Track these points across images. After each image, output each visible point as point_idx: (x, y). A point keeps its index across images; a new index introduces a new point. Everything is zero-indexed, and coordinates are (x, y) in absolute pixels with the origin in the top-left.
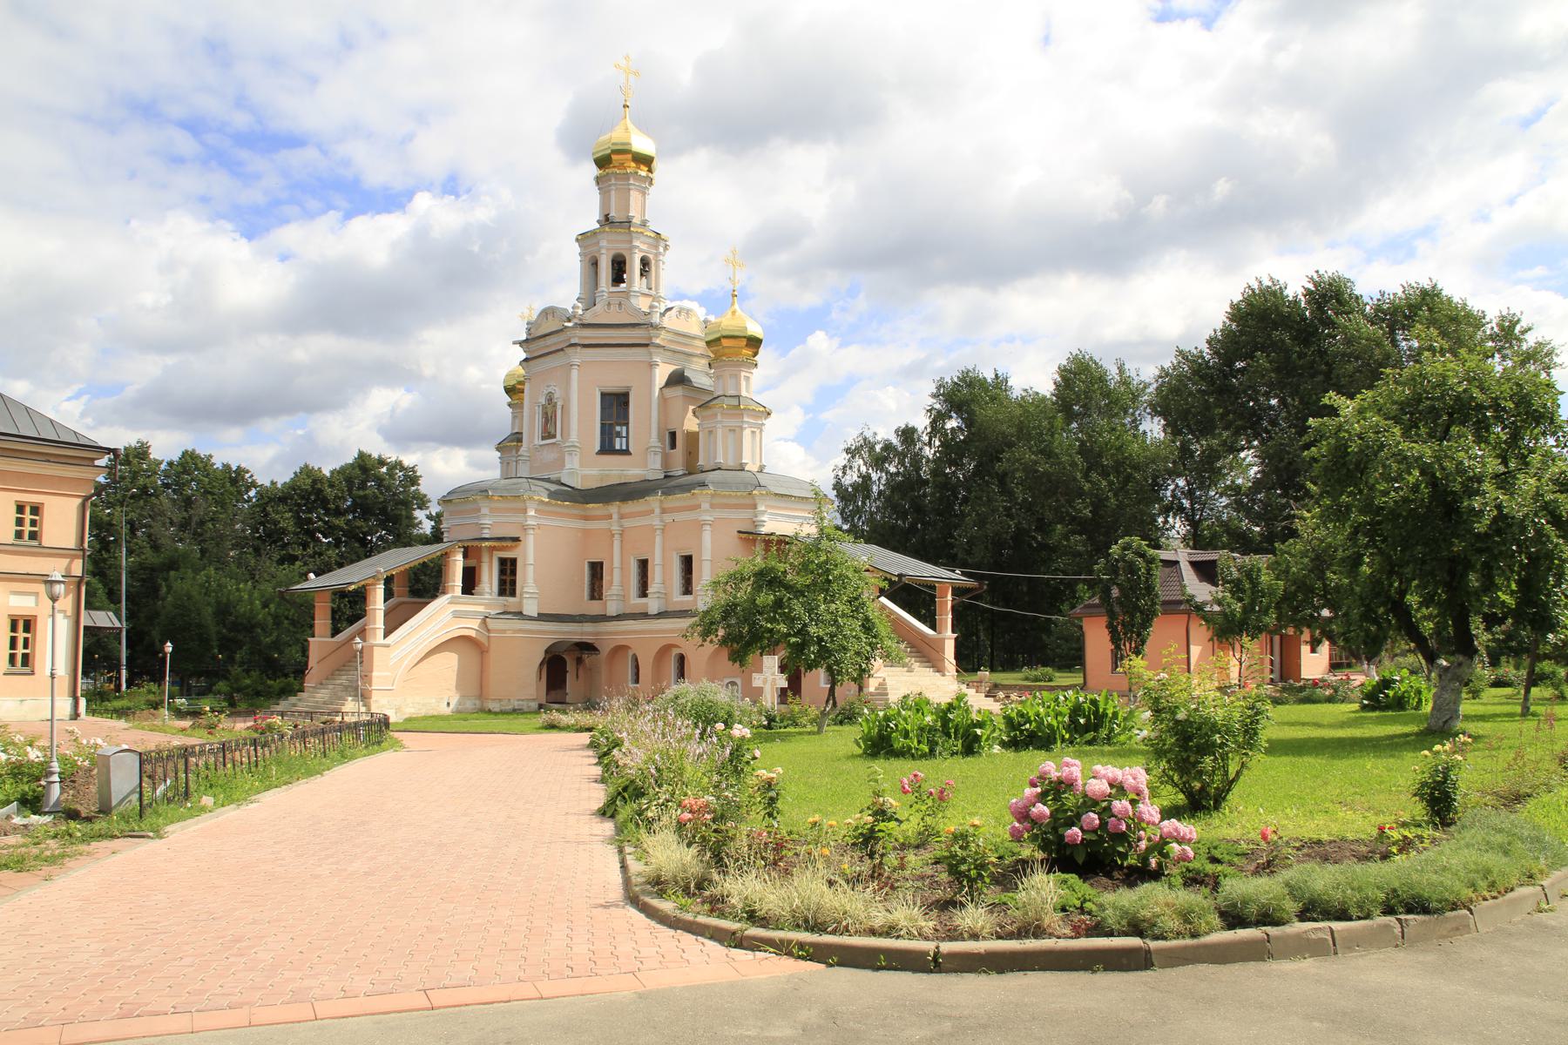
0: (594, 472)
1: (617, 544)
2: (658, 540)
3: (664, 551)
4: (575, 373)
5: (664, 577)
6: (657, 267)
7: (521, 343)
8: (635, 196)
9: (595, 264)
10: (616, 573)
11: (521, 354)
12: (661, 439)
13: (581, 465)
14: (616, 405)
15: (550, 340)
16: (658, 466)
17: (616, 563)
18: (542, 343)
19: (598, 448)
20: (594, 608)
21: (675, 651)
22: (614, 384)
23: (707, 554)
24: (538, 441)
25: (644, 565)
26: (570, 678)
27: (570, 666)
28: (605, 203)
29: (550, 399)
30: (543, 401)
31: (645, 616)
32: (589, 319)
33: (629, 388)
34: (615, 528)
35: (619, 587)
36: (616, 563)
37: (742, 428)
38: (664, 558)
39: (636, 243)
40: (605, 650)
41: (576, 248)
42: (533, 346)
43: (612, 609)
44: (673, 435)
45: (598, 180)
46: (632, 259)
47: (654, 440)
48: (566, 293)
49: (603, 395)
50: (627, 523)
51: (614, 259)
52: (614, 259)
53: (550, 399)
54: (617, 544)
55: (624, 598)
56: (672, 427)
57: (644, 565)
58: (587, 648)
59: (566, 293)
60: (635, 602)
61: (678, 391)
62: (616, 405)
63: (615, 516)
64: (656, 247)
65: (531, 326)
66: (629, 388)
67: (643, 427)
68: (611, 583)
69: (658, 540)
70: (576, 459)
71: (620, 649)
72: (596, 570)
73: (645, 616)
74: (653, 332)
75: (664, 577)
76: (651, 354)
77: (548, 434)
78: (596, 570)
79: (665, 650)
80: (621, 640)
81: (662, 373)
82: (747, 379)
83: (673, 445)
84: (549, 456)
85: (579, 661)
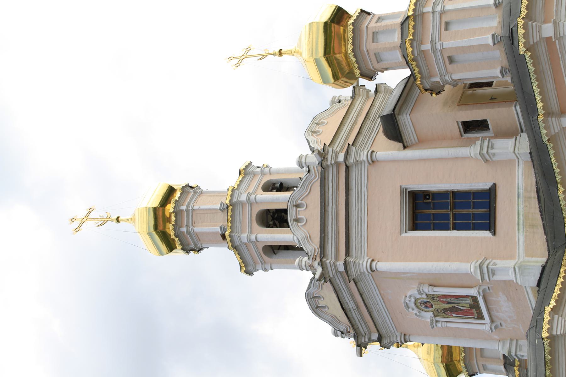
0: (521, 238)
4: (382, 266)
6: (278, 172)
7: (361, 346)
8: (201, 204)
9: (274, 250)
11: (374, 347)
12: (471, 143)
13: (511, 257)
14: (427, 210)
15: (351, 305)
16: (510, 142)
18: (354, 315)
19: (486, 234)
22: (394, 211)
24: (485, 325)
28: (213, 243)
29: (425, 304)
30: (428, 316)
32: (312, 247)
33: (403, 191)
37: (443, 12)
39: (243, 198)
41: (259, 274)
42: (362, 329)
44: (469, 127)
45: (187, 250)
46: (262, 202)
47: (473, 151)
48: (291, 282)
49: (415, 226)
51: (264, 224)
52: (264, 224)
53: (425, 304)
56: (455, 129)
59: (291, 282)
61: (406, 121)
62: (427, 210)
64: (255, 174)
65: (340, 333)
66: (403, 191)
67: (451, 168)
70: (501, 264)
74: (330, 160)
76: (358, 163)
77: (473, 310)
81: (386, 149)
82: (380, 19)
83: (479, 126)
84: (504, 307)
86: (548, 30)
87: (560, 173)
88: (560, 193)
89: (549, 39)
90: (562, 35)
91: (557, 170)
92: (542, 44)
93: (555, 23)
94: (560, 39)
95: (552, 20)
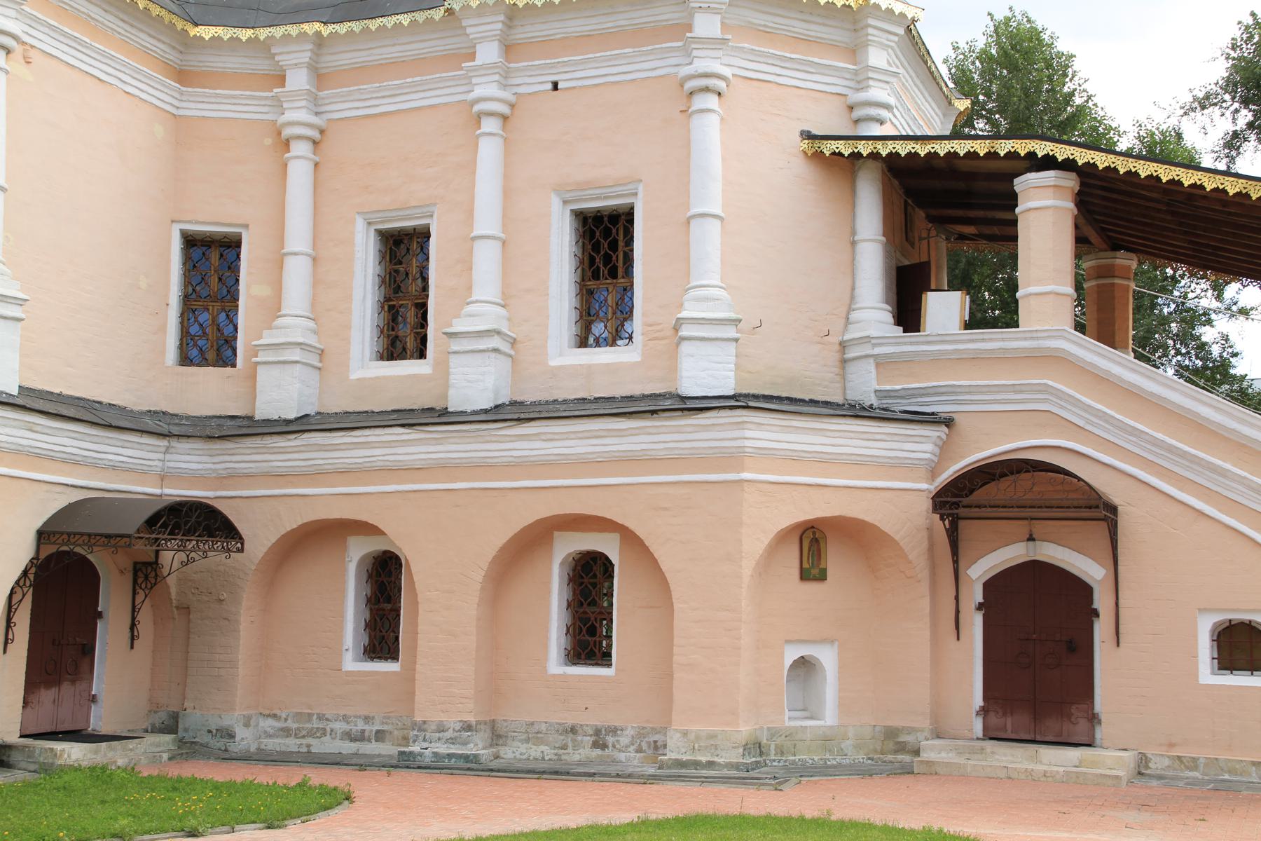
1: (299, 173)
2: (489, 152)
3: (508, 193)
5: (505, 297)
10: (297, 274)
17: (298, 235)
20: (208, 391)
21: (570, 545)
23: (711, 195)
25: (403, 252)
26: (109, 637)
27: (113, 599)
31: (437, 416)
34: (297, 115)
35: (310, 321)
36: (298, 235)
38: (507, 218)
40: (260, 533)
43: (280, 394)
50: (343, 105)
54: (299, 173)
55: (322, 359)
57: (403, 252)
58: (201, 523)
60: (371, 376)
63: (298, 80)
68: (274, 308)
69: (489, 152)
71: (324, 534)
72: (211, 262)
73: (437, 416)
75: (505, 297)
78: (211, 262)
79: (537, 536)
80: (328, 501)
85: (145, 574)
86: (706, 26)
87: (366, 30)
88: (317, 26)
89: (689, 28)
90: (695, 53)
91: (373, 25)
92: (677, 15)
93: (724, 41)
94: (687, 52)
95: (729, 37)
